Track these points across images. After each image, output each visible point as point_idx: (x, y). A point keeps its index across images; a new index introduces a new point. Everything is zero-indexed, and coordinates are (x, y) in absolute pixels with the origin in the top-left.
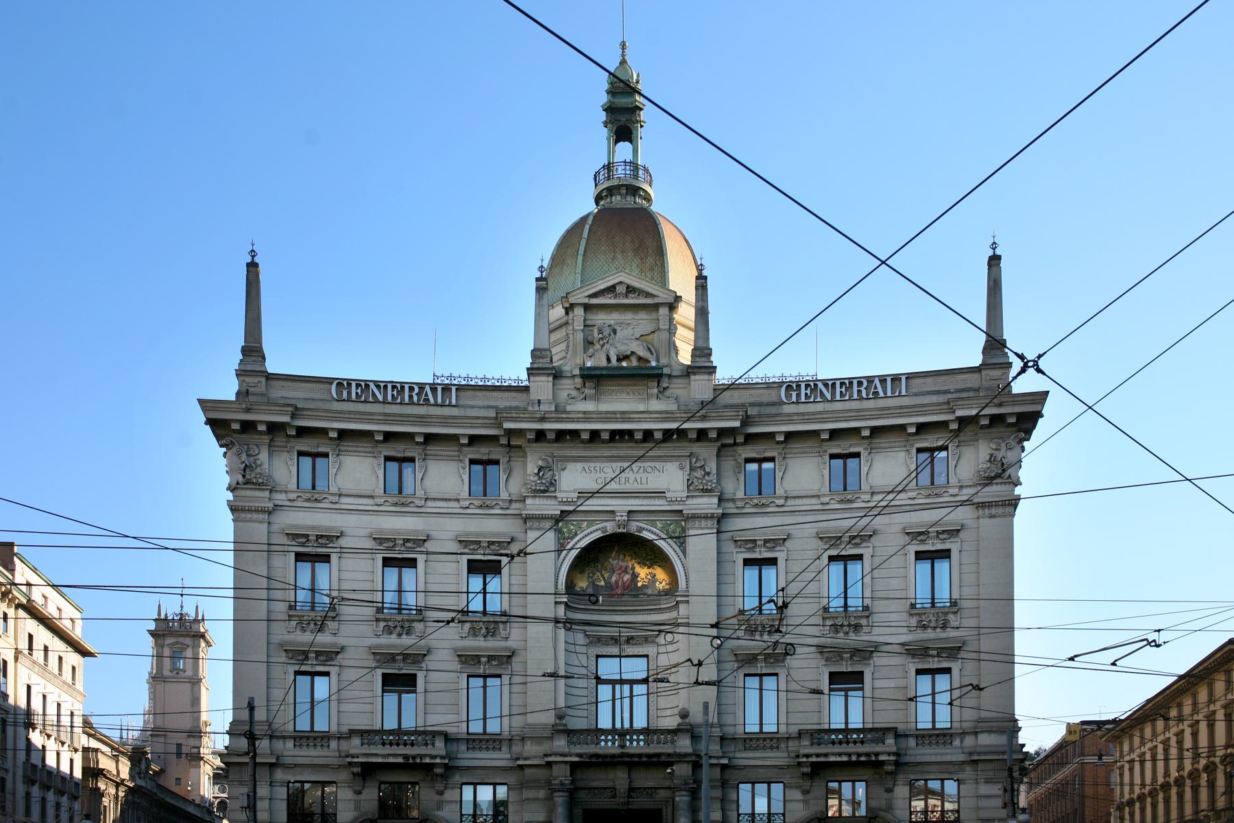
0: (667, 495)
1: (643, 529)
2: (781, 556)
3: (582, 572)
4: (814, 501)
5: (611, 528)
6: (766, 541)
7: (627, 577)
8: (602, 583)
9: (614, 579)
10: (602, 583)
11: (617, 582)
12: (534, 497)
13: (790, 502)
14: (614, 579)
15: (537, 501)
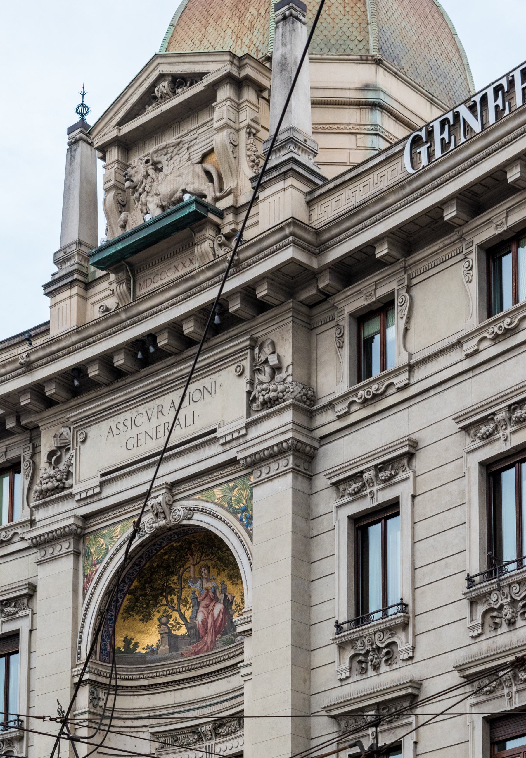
0: (218, 434)
1: (193, 510)
2: (402, 491)
3: (147, 618)
4: (457, 355)
5: (150, 523)
6: (379, 468)
7: (218, 608)
8: (183, 631)
9: (200, 617)
10: (183, 631)
11: (205, 623)
12: (45, 504)
13: (419, 374)
14: (200, 617)
15: (51, 510)
